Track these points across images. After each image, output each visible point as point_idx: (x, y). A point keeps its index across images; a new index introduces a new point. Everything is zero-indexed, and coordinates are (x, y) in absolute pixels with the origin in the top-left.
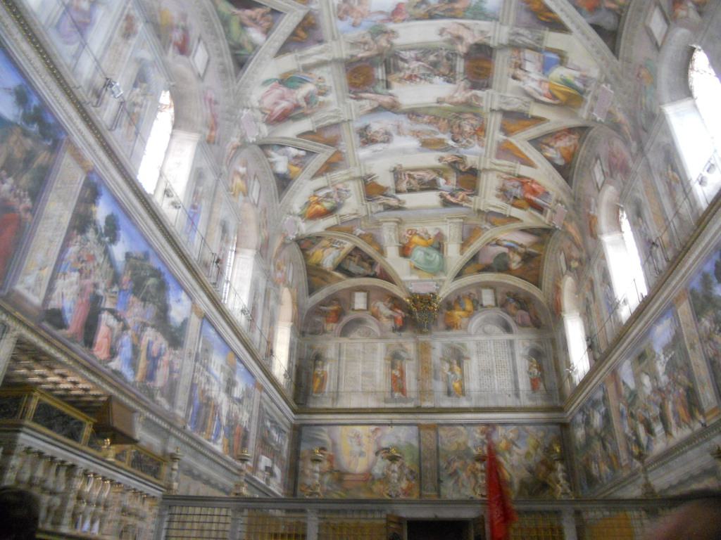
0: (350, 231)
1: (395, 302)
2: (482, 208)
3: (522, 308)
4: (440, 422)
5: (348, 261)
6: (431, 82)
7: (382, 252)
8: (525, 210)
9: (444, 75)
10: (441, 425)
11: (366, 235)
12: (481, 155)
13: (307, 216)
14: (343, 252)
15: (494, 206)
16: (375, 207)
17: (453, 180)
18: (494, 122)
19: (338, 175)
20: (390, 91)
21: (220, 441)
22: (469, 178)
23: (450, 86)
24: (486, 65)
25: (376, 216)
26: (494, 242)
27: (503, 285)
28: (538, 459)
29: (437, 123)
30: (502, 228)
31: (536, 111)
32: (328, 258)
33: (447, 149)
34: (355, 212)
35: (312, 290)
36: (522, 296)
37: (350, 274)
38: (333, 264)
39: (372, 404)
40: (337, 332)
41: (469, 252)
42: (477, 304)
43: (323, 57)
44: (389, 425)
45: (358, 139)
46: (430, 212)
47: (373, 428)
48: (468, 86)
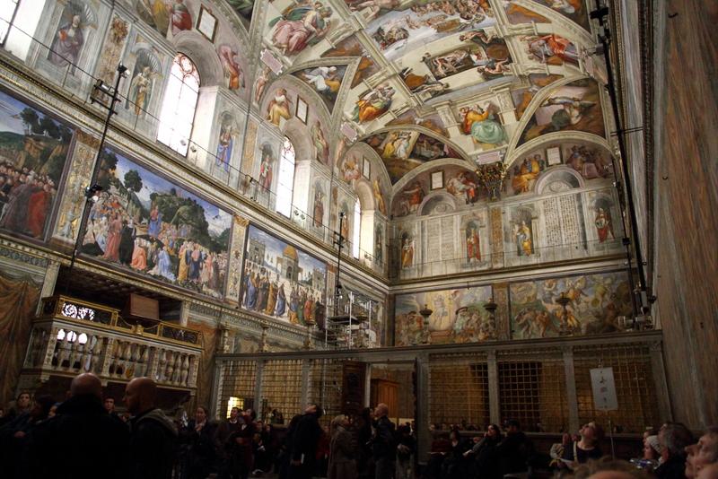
0: (412, 122)
1: (467, 176)
2: (521, 73)
3: (588, 161)
4: (511, 279)
5: (418, 148)
7: (445, 133)
8: (560, 65)
10: (512, 282)
11: (425, 122)
13: (361, 119)
14: (411, 141)
15: (532, 69)
16: (423, 96)
17: (484, 54)
19: (375, 78)
21: (286, 314)
22: (498, 48)
25: (428, 102)
26: (547, 102)
27: (568, 141)
28: (605, 305)
29: (441, 7)
32: (402, 149)
34: (405, 105)
35: (394, 180)
36: (587, 148)
37: (426, 159)
38: (406, 152)
39: (451, 270)
41: (526, 118)
42: (544, 165)
44: (464, 287)
45: (376, 43)
46: (475, 88)
47: (453, 291)
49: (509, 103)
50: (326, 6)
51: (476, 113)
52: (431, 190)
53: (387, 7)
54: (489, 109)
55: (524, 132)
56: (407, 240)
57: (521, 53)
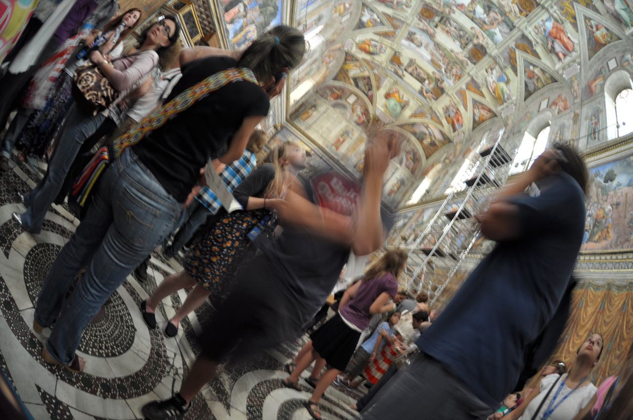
0: (373, 69)
1: (366, 112)
2: (433, 108)
6: (454, 41)
7: (378, 88)
8: (448, 123)
9: (460, 42)
14: (361, 74)
16: (391, 68)
17: (432, 86)
18: (466, 79)
19: (387, 42)
20: (435, 29)
22: (439, 91)
23: (460, 50)
24: (480, 56)
27: (414, 145)
29: (444, 57)
30: (434, 123)
31: (484, 90)
32: (354, 72)
33: (440, 71)
35: (335, 79)
37: (357, 86)
41: (414, 120)
51: (399, 96)
52: (346, 100)
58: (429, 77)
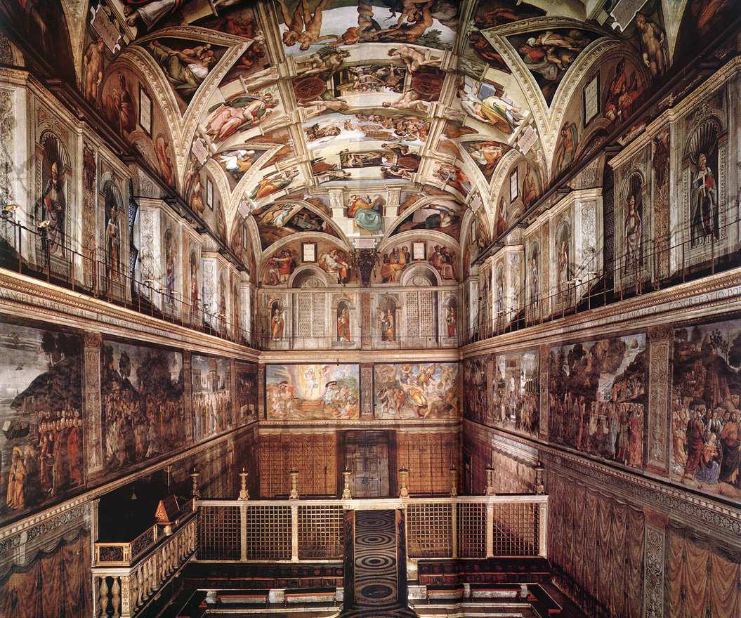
0: (301, 197)
2: (419, 181)
6: (377, 91)
7: (329, 212)
11: (313, 199)
12: (421, 147)
15: (430, 182)
17: (395, 160)
19: (286, 163)
20: (339, 98)
22: (412, 162)
23: (400, 95)
26: (428, 206)
27: (433, 239)
34: (302, 184)
36: (447, 250)
37: (301, 229)
40: (290, 281)
41: (405, 214)
42: (410, 257)
43: (270, 78)
46: (371, 182)
47: (323, 366)
48: (413, 96)
49: (396, 200)
50: (275, 99)
52: (303, 261)
53: (334, 109)
54: (376, 201)
55: (400, 225)
56: (277, 311)
57: (429, 169)
58: (382, 154)
